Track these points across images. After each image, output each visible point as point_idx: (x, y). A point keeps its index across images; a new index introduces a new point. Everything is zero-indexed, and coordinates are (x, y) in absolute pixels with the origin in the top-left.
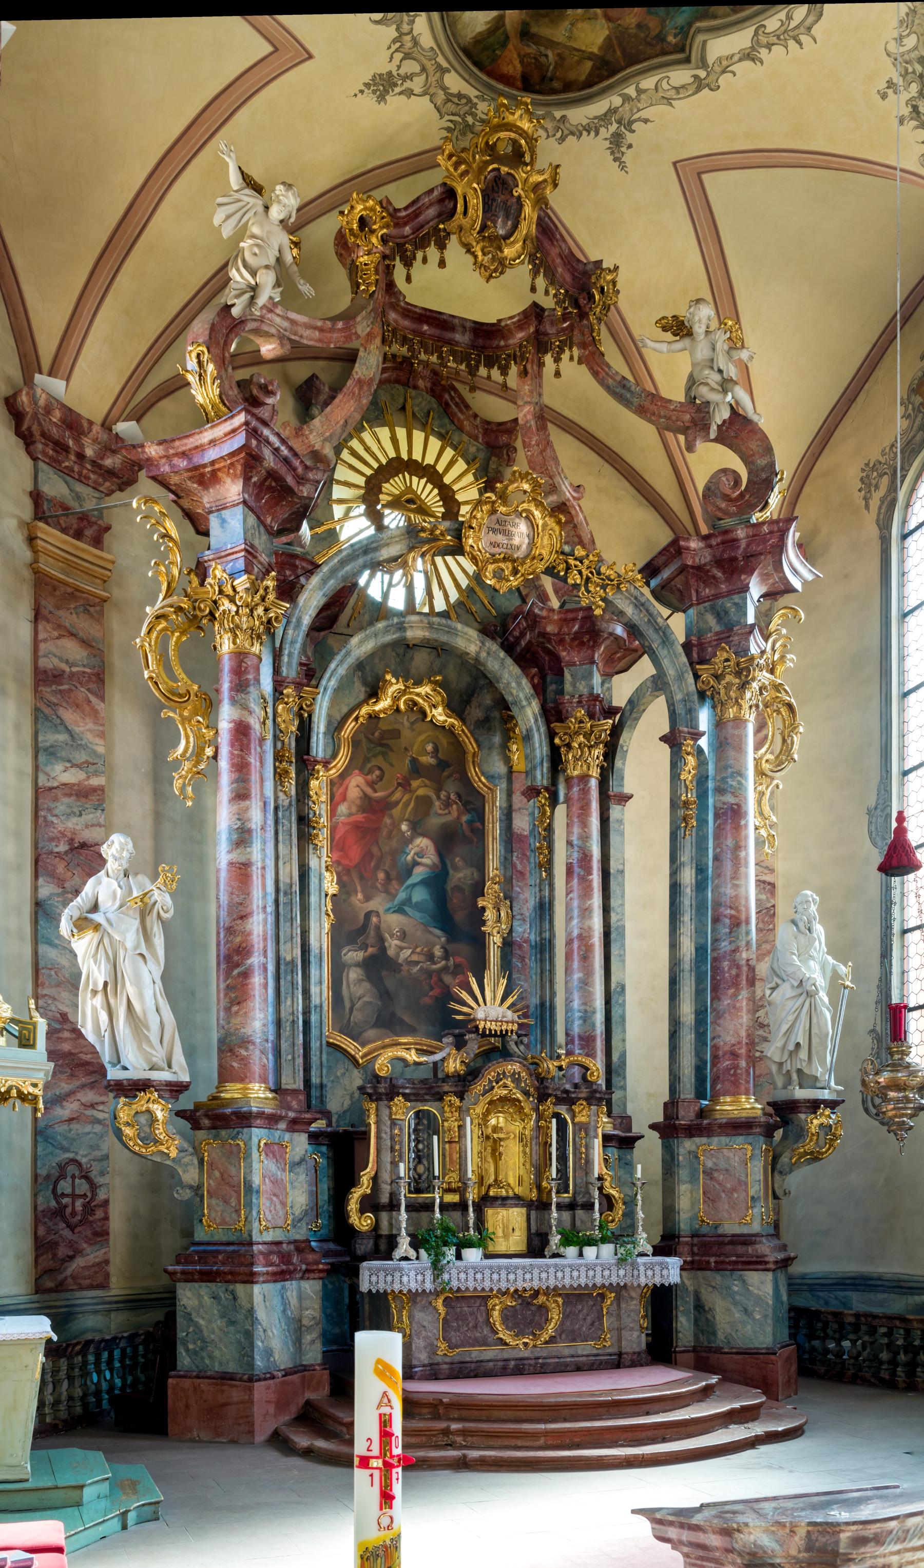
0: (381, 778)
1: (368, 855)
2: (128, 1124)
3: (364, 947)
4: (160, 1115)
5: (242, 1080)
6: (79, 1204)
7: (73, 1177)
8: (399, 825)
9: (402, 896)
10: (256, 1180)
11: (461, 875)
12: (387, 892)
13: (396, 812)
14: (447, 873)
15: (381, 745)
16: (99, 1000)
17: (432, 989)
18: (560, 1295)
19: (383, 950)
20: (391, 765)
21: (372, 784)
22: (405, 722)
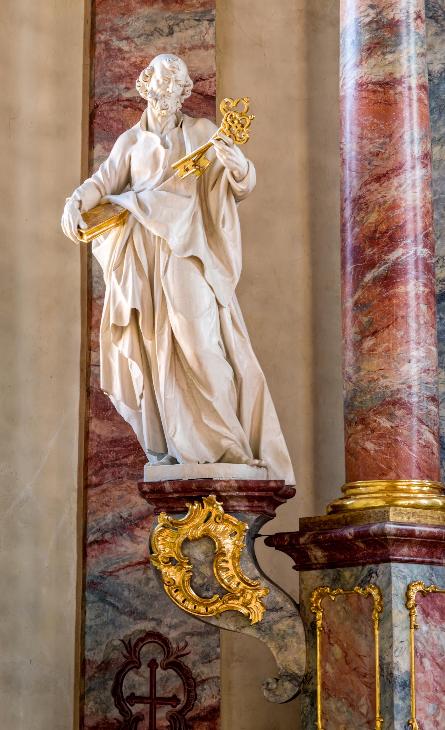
2: (171, 561)
4: (228, 544)
5: (381, 475)
6: (162, 714)
7: (153, 665)
10: (402, 663)
16: (125, 345)
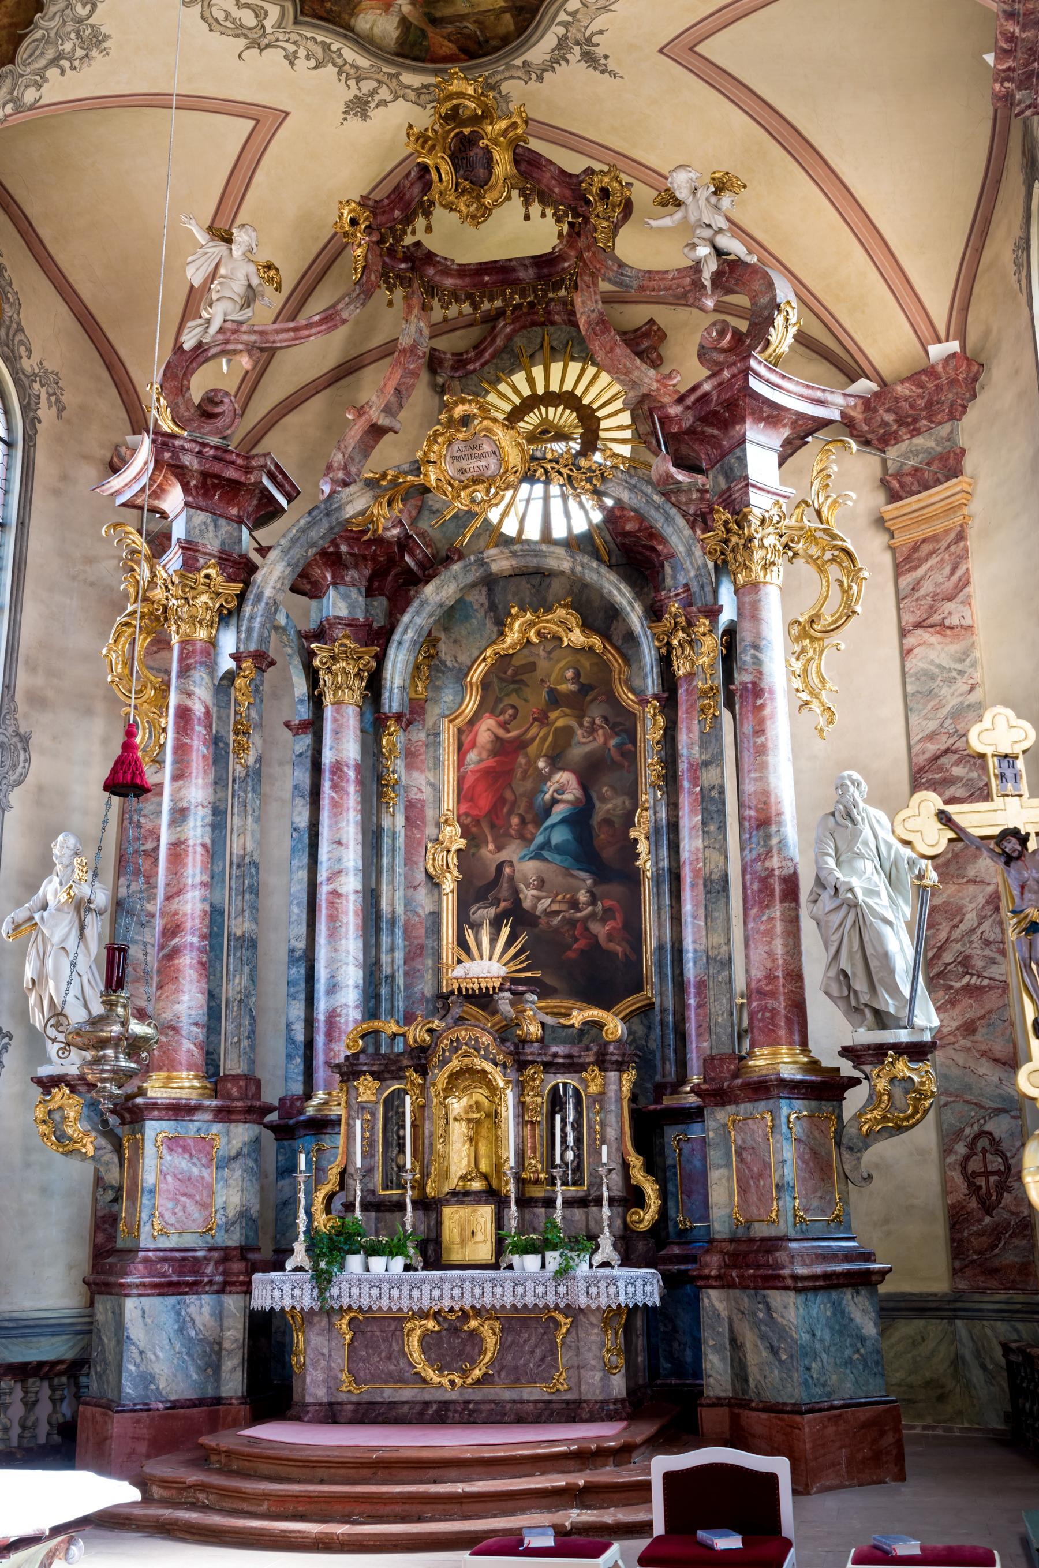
0: (514, 717)
1: (501, 800)
3: (496, 902)
8: (536, 762)
9: (539, 839)
11: (610, 806)
12: (522, 837)
13: (532, 749)
14: (593, 806)
15: (514, 682)
17: (576, 940)
18: (498, 1318)
19: (517, 902)
20: (526, 700)
21: (503, 725)
22: (542, 653)
